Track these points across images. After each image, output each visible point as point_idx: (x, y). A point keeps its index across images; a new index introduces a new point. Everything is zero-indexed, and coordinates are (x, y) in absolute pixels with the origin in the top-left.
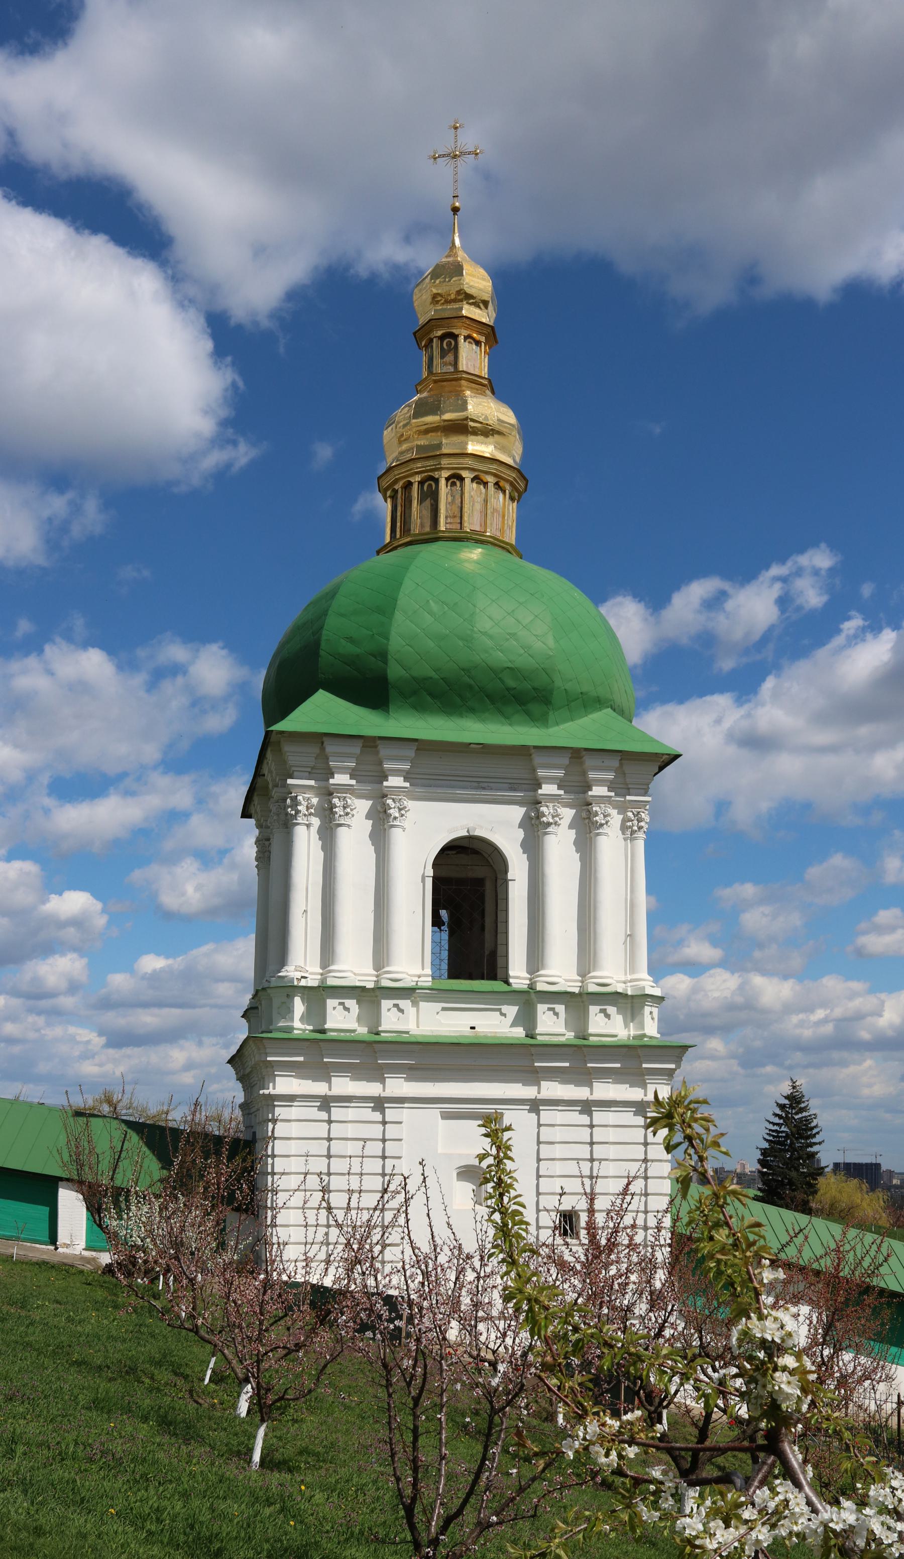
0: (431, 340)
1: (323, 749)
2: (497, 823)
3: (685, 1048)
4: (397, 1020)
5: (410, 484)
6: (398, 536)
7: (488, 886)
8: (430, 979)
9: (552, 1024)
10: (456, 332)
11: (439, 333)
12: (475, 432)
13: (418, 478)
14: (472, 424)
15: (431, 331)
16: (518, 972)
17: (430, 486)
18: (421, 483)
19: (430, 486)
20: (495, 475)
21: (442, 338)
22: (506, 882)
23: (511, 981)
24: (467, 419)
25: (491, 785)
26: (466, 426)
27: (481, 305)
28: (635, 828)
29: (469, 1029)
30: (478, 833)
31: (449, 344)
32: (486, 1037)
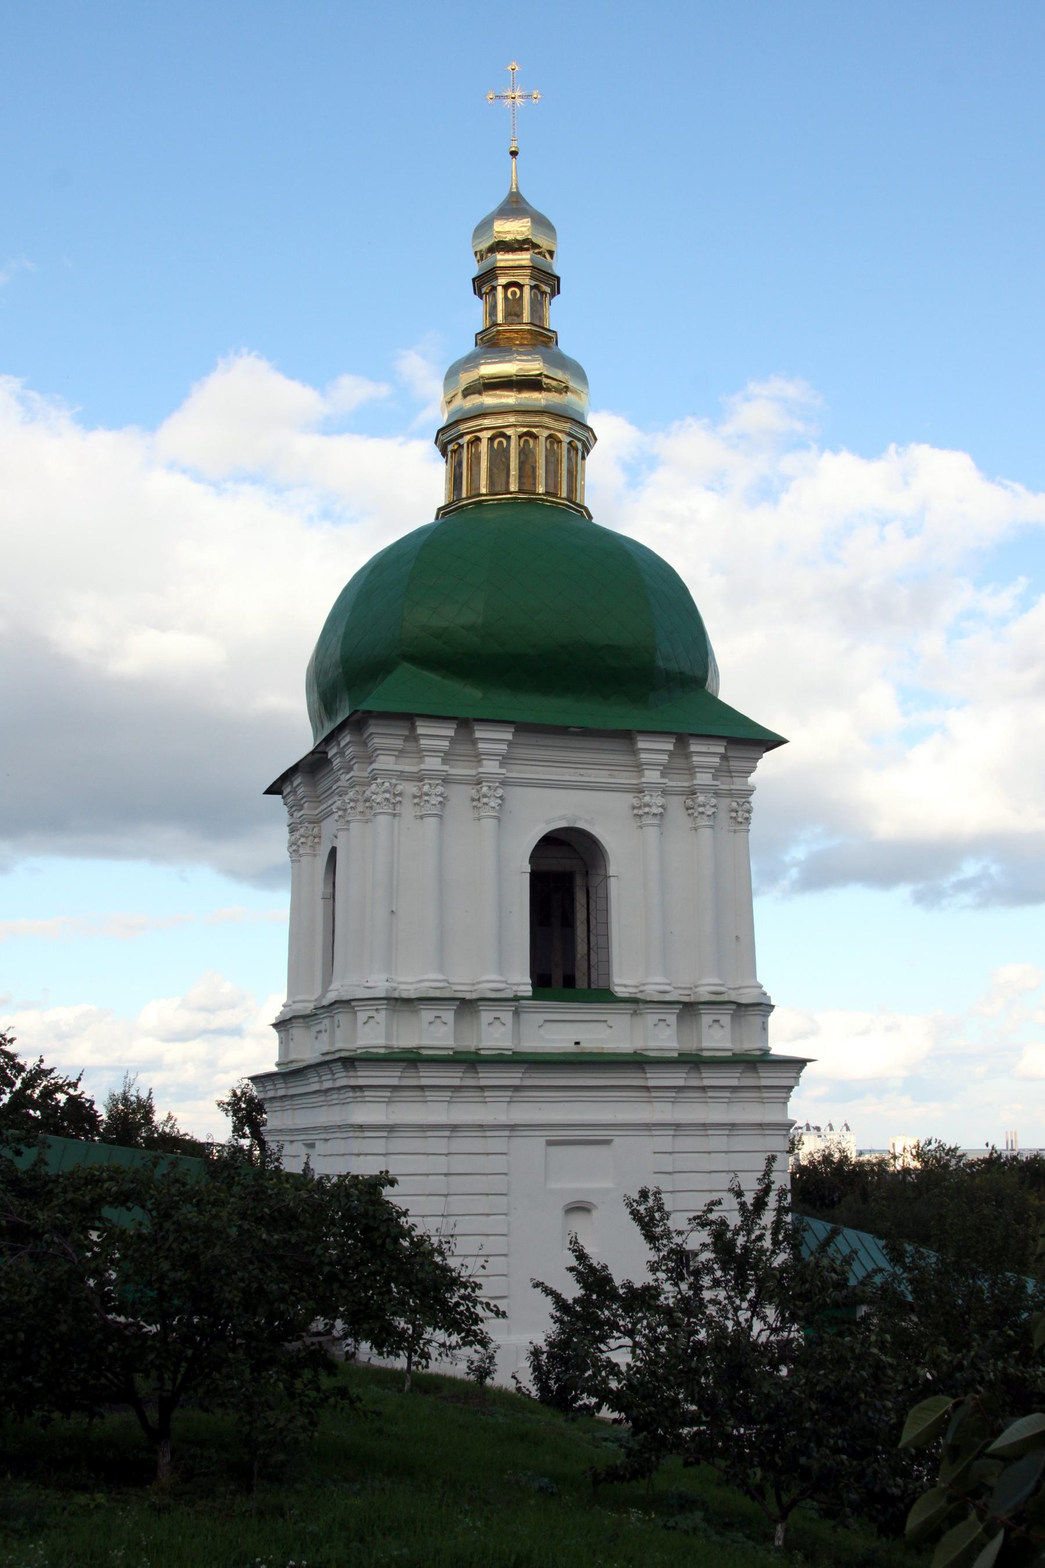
0: (494, 288)
1: (413, 728)
3: (801, 1063)
4: (494, 1034)
5: (478, 439)
6: (464, 495)
7: (579, 881)
8: (530, 988)
10: (521, 282)
11: (502, 281)
12: (548, 389)
13: (489, 434)
14: (546, 380)
15: (496, 278)
16: (623, 979)
17: (501, 443)
18: (491, 439)
19: (501, 443)
20: (569, 435)
21: (506, 287)
22: (607, 877)
23: (617, 989)
24: (540, 375)
25: (614, 773)
26: (540, 382)
27: (547, 256)
28: (740, 820)
29: (573, 1045)
30: (580, 825)
31: (514, 294)
32: (591, 1054)
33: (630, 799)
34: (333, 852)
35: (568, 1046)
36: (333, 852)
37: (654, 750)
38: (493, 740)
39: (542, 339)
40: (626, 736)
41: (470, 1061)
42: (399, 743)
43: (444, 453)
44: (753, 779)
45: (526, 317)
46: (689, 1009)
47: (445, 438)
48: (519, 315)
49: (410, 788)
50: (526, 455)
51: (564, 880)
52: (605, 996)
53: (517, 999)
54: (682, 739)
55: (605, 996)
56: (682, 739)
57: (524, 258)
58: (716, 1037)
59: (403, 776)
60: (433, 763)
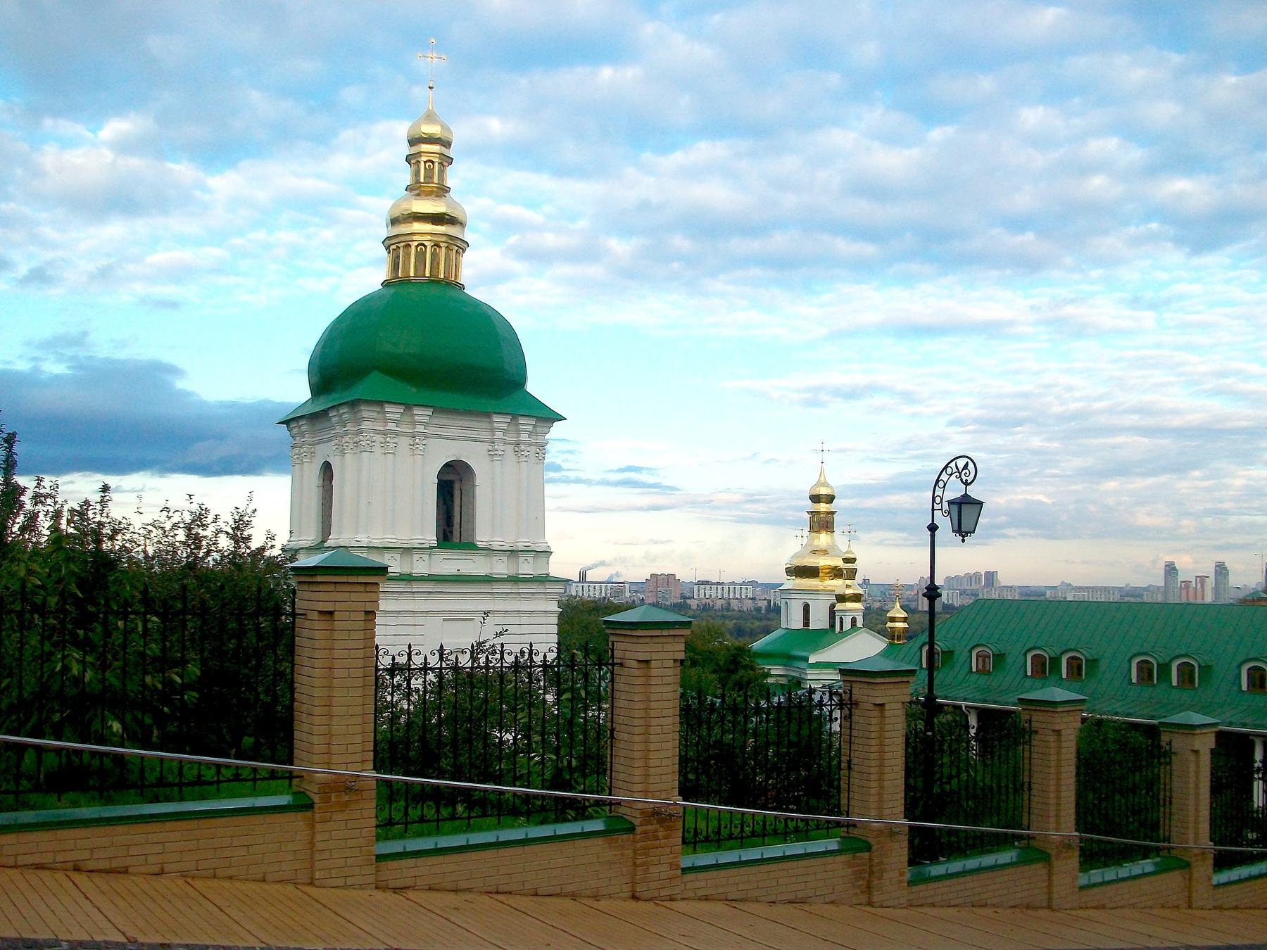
2: (473, 454)
7: (457, 486)
9: (501, 568)
11: (424, 159)
16: (481, 538)
22: (474, 486)
33: (486, 446)
34: (327, 468)
35: (454, 572)
36: (327, 468)
37: (501, 421)
38: (422, 414)
39: (442, 191)
40: (487, 415)
41: (514, 579)
42: (374, 415)
43: (387, 248)
44: (547, 437)
45: (436, 180)
46: (513, 553)
47: (388, 242)
48: (432, 178)
49: (379, 438)
50: (434, 256)
51: (453, 485)
52: (471, 546)
53: (431, 548)
54: (514, 417)
55: (471, 546)
56: (514, 417)
57: (436, 148)
58: (526, 568)
59: (375, 432)
60: (391, 426)
